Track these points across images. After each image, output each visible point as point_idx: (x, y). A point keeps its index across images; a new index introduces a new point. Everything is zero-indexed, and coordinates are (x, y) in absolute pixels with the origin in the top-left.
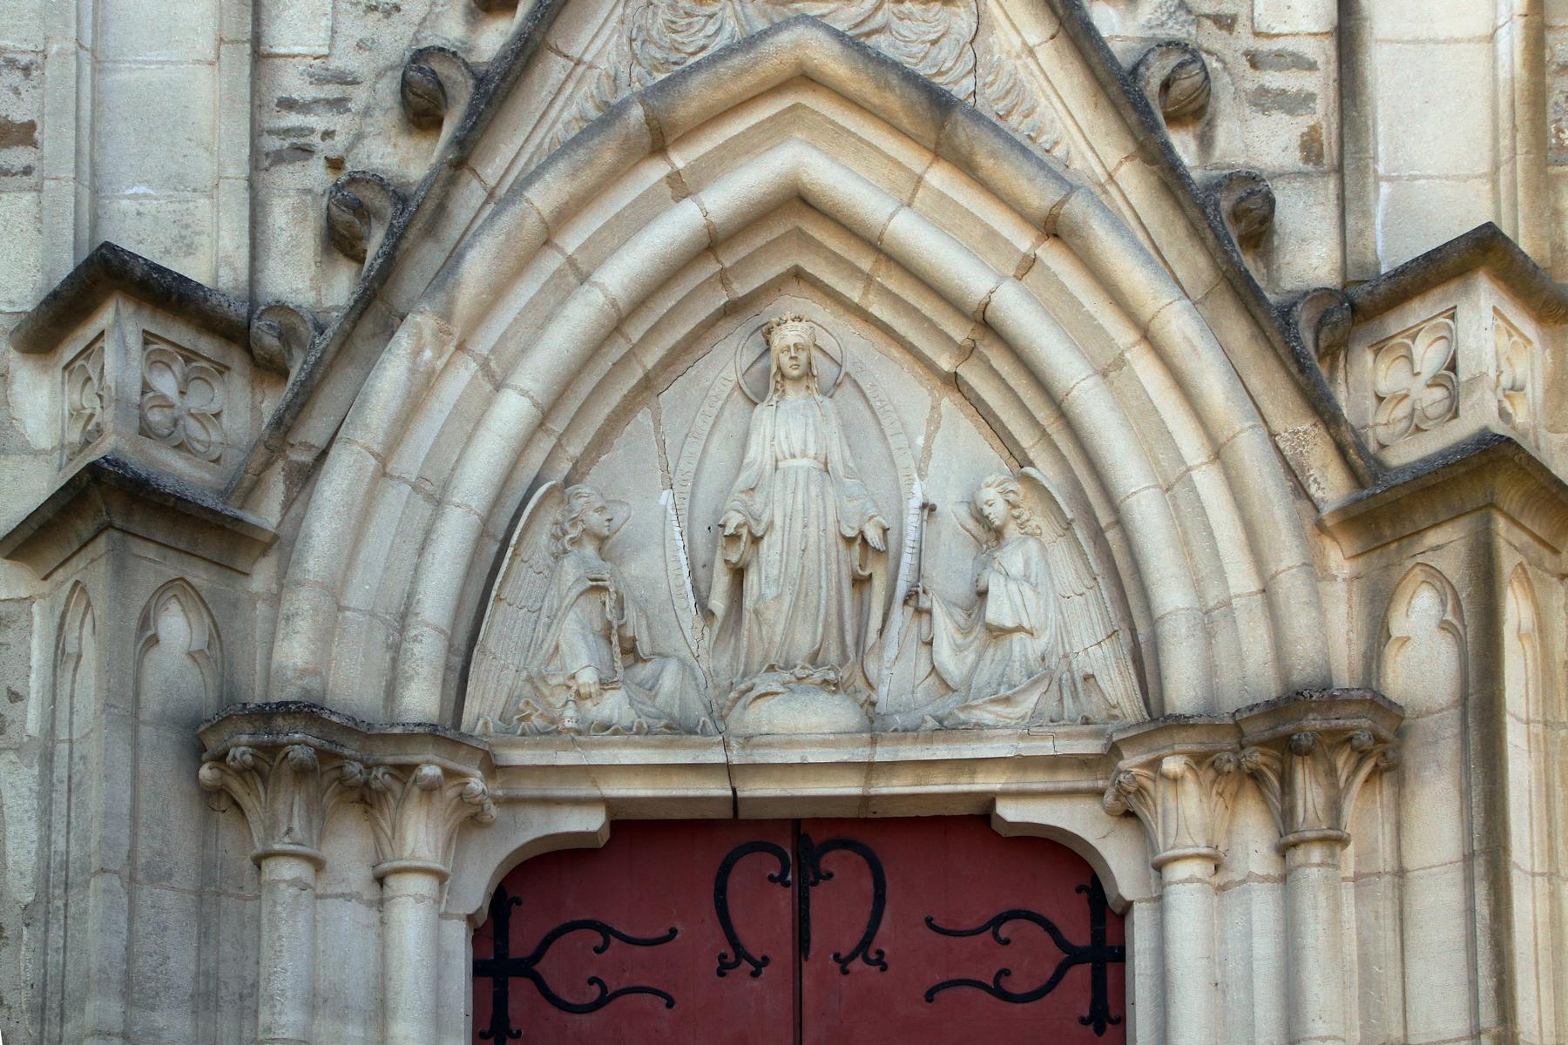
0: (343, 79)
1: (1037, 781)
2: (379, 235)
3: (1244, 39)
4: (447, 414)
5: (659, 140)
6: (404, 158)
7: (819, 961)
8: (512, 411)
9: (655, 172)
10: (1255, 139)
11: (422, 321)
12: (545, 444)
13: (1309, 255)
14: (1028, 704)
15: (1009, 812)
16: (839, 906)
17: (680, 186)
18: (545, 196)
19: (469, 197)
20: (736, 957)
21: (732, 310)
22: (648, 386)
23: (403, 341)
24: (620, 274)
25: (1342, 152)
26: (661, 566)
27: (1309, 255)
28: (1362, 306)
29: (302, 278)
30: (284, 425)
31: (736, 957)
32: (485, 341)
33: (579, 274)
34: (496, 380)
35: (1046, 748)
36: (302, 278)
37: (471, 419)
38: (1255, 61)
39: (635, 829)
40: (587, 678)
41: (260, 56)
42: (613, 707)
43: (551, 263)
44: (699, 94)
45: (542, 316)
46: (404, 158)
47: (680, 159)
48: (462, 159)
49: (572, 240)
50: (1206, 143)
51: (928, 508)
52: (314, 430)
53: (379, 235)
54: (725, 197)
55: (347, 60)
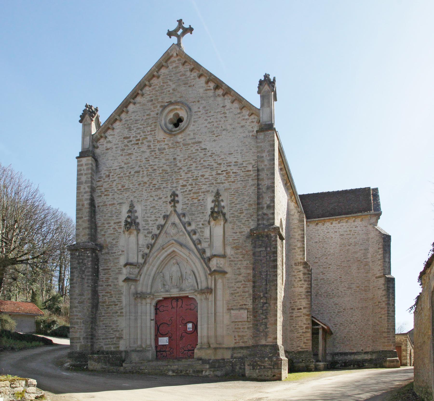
0: (144, 245)
1: (191, 294)
2: (145, 256)
3: (204, 237)
4: (151, 269)
5: (163, 249)
6: (147, 251)
7: (178, 308)
8: (155, 269)
9: (164, 251)
10: (205, 245)
11: (147, 264)
12: (158, 270)
13: (208, 254)
14: (190, 288)
15: (189, 296)
16: (180, 303)
17: (166, 251)
18: (155, 254)
19: (151, 254)
20: (173, 308)
21: (172, 258)
22: (166, 264)
23: (146, 266)
24: (161, 259)
25: (211, 245)
26: (167, 278)
27: (208, 254)
28: (209, 259)
29: (141, 261)
30: (139, 272)
31: (173, 308)
32: (152, 264)
33: (159, 258)
34: (154, 266)
35: (190, 292)
36: (141, 261)
37: (152, 270)
38: (205, 239)
39: (165, 299)
40: (160, 288)
41: (138, 244)
42: (162, 290)
43: (157, 258)
44: (165, 246)
45: (164, 253)
46: (147, 251)
47: (165, 250)
48: (150, 252)
49: (158, 256)
50: (201, 246)
51: (186, 272)
52: (141, 272)
53: (145, 256)
54: (168, 252)
55: (144, 244)
